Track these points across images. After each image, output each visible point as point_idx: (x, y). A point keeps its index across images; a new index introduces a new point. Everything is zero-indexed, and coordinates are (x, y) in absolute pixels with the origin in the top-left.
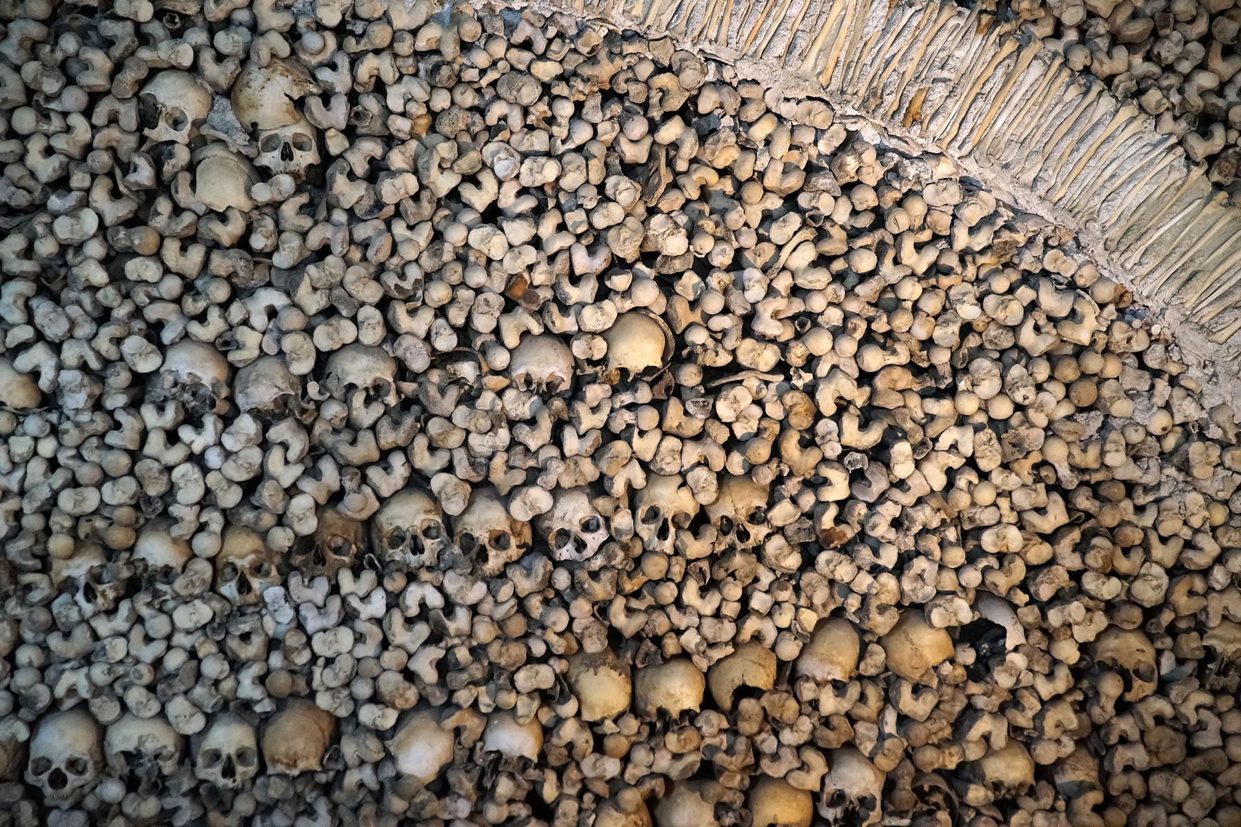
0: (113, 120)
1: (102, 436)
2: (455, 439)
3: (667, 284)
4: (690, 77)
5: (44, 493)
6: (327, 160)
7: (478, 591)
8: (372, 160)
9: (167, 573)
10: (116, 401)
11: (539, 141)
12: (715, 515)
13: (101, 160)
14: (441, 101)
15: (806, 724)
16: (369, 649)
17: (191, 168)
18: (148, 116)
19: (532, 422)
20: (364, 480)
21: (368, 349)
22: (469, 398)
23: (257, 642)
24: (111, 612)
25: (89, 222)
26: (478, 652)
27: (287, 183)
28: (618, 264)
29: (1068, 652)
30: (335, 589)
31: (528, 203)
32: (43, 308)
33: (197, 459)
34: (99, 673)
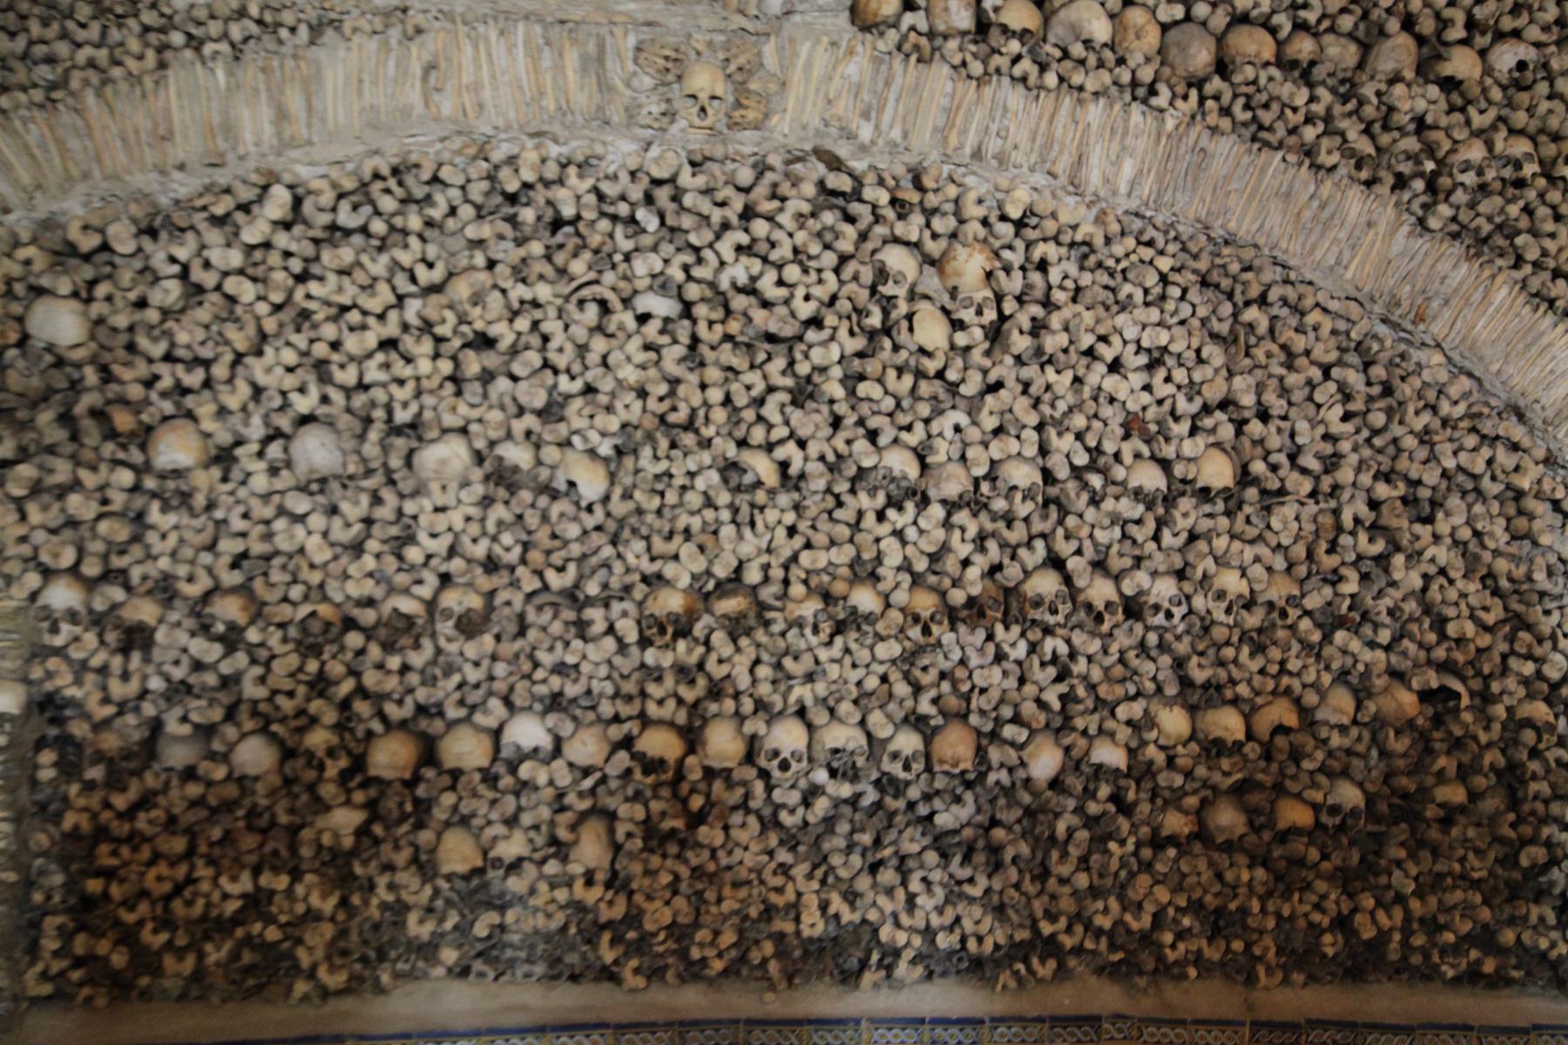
0: (856, 278)
1: (830, 513)
2: (1085, 532)
3: (1240, 425)
4: (1267, 276)
5: (786, 553)
6: (1003, 318)
7: (1095, 646)
8: (1034, 319)
9: (870, 618)
10: (842, 487)
11: (1154, 314)
12: (1261, 600)
13: (844, 305)
14: (1086, 279)
15: (1320, 755)
16: (1012, 683)
17: (910, 317)
18: (882, 274)
19: (1139, 522)
20: (1013, 557)
21: (1026, 459)
22: (1095, 501)
23: (932, 676)
24: (829, 643)
25: (835, 352)
26: (1092, 687)
27: (978, 333)
28: (1207, 409)
29: (1499, 711)
30: (990, 637)
31: (1143, 360)
32: (796, 415)
33: (899, 534)
34: (821, 688)
